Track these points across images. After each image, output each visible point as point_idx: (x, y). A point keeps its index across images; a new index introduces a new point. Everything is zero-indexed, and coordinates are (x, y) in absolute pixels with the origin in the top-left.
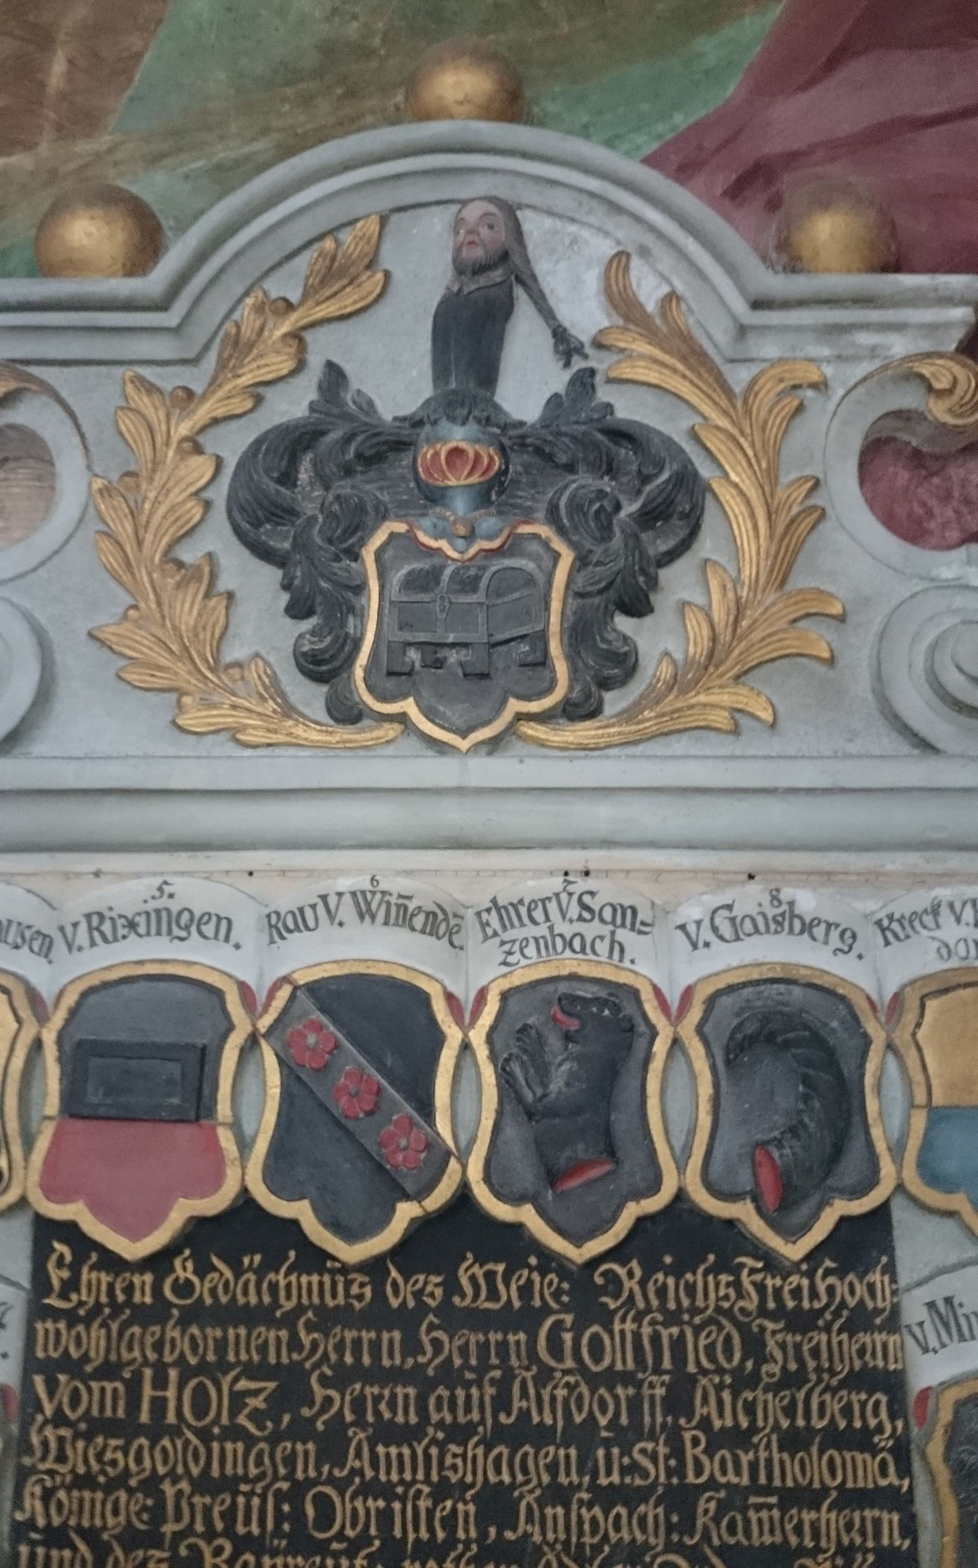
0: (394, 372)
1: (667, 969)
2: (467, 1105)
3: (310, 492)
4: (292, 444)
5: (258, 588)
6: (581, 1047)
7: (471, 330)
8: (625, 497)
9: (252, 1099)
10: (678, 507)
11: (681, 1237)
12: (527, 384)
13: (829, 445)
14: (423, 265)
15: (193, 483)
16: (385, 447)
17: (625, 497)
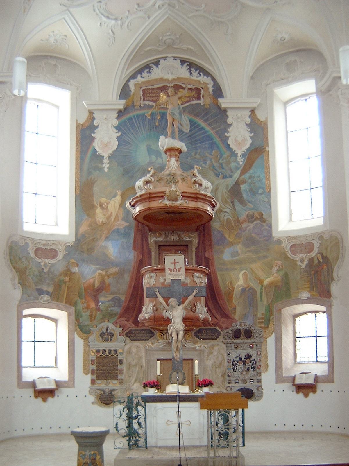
0: (105, 331)
1: (112, 349)
2: (107, 353)
3: (102, 335)
4: (101, 334)
5: (101, 338)
6: (110, 351)
7: (107, 330)
8: (112, 335)
9: (101, 352)
10: (113, 335)
11: (112, 355)
12: (109, 331)
13: (118, 333)
14: (105, 327)
15: (99, 334)
16: (104, 333)
17: (112, 335)
